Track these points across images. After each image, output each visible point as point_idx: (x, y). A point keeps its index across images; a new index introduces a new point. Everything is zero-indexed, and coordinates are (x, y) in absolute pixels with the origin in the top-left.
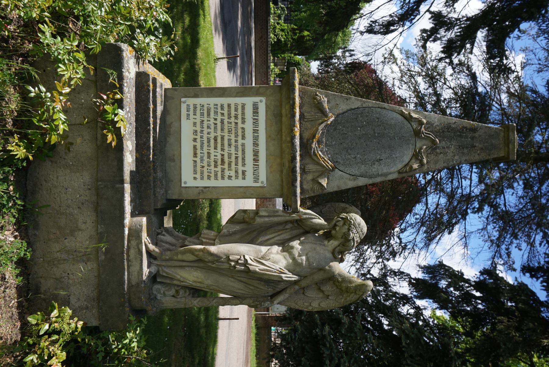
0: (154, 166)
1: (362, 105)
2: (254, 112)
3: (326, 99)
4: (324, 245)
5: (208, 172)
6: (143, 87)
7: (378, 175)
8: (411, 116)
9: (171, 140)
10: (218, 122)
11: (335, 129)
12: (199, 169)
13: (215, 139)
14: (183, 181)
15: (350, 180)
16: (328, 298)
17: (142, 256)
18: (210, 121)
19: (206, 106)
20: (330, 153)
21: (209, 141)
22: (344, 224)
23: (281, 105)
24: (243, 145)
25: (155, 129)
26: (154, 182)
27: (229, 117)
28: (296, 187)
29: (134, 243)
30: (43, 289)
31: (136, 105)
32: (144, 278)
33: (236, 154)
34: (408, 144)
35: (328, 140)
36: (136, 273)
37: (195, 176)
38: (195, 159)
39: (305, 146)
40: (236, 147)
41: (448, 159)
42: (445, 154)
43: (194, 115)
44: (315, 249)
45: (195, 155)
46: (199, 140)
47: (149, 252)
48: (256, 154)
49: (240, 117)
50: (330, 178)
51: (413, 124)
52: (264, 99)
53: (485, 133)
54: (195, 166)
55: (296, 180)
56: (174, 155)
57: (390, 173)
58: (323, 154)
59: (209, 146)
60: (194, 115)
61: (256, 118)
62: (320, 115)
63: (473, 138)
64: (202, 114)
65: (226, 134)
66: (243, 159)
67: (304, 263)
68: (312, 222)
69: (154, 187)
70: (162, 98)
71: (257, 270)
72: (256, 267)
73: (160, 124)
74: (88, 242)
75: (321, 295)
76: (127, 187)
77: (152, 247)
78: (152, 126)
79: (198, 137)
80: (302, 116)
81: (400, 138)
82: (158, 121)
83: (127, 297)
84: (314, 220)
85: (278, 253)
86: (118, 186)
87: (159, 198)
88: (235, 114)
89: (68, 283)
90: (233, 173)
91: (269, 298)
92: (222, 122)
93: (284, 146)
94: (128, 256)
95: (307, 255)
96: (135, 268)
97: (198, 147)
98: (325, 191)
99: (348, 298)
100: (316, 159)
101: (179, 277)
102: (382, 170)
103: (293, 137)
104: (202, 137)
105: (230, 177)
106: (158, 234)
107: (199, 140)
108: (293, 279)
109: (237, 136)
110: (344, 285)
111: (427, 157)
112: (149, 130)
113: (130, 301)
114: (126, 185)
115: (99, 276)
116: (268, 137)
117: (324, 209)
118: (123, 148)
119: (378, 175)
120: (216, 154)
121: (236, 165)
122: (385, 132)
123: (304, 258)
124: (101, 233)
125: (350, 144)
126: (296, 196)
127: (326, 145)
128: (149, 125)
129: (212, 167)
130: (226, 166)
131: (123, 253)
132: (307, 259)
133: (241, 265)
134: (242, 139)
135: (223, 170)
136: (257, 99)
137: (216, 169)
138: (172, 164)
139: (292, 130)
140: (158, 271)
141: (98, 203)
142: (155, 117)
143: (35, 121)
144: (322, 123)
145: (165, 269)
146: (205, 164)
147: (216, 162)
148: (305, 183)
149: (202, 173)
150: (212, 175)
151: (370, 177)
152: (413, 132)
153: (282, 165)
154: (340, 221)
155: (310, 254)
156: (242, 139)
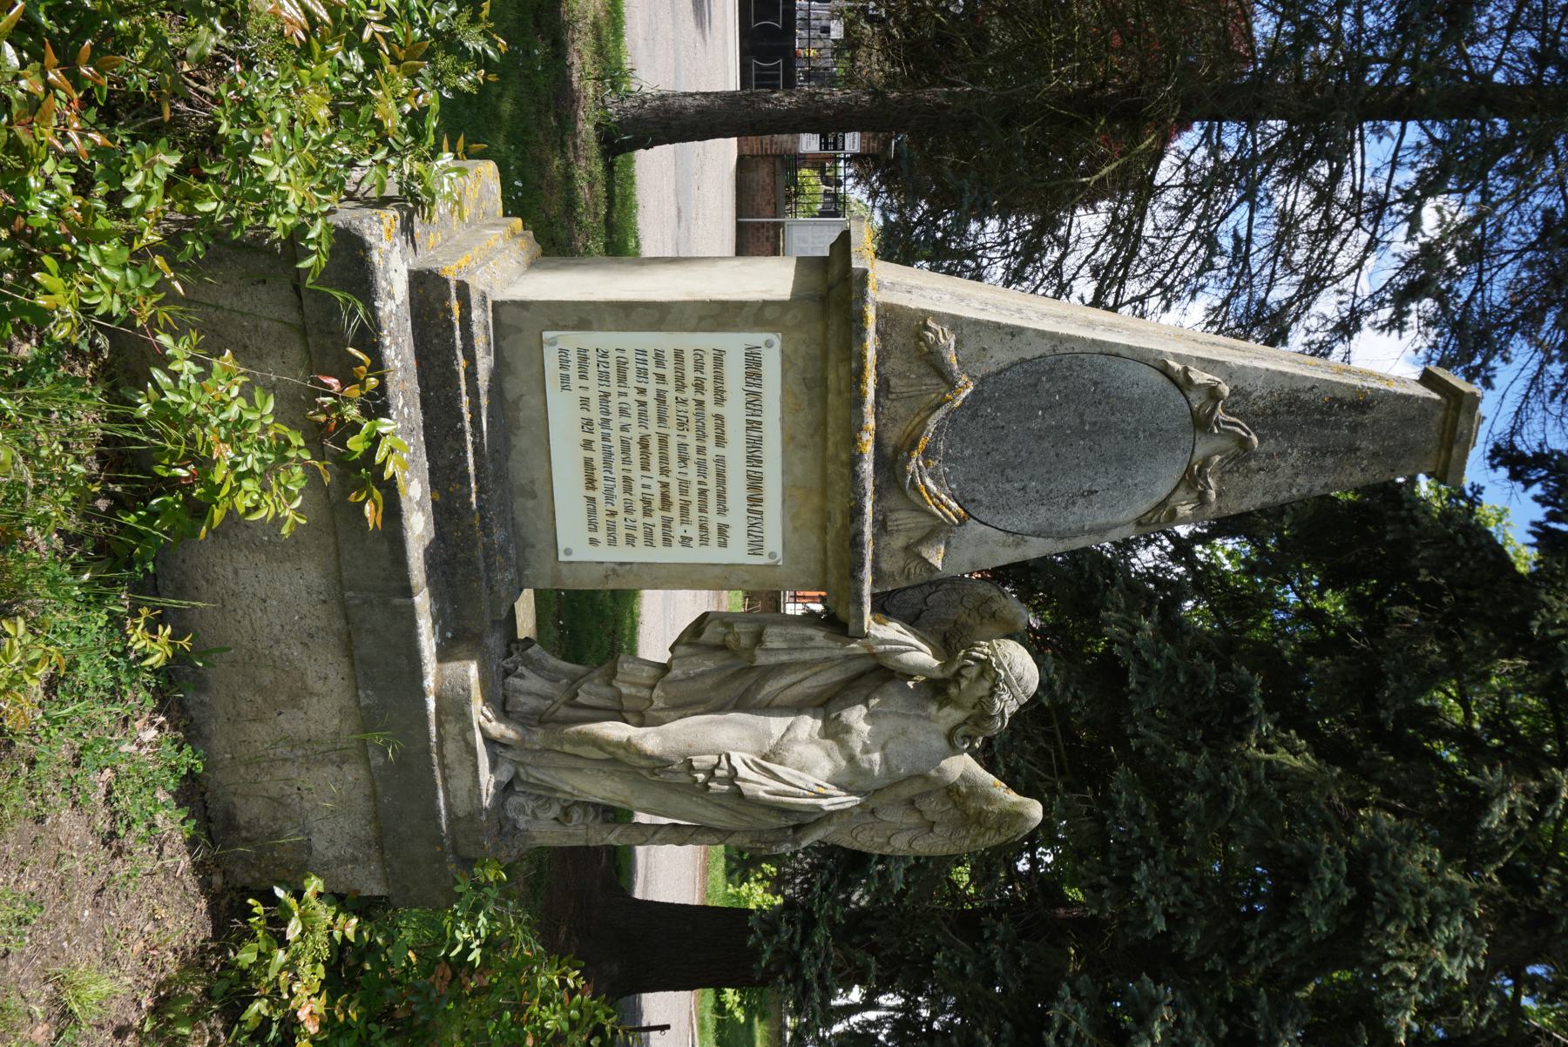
0: (482, 518)
1: (1054, 348)
2: (748, 375)
3: (952, 340)
4: (928, 718)
5: (627, 527)
6: (434, 313)
7: (1082, 531)
8: (1189, 380)
9: (522, 441)
10: (650, 398)
11: (974, 417)
12: (602, 518)
13: (644, 443)
14: (561, 547)
15: (1004, 545)
16: (932, 830)
17: (475, 756)
18: (626, 394)
19: (613, 355)
20: (956, 480)
21: (626, 449)
22: (981, 675)
23: (825, 356)
24: (720, 461)
25: (475, 422)
26: (486, 557)
27: (681, 387)
28: (862, 582)
29: (452, 728)
30: (242, 819)
31: (419, 365)
32: (486, 802)
33: (700, 483)
34: (1173, 450)
35: (951, 446)
36: (465, 793)
37: (593, 535)
38: (591, 494)
39: (890, 465)
40: (701, 465)
41: (1278, 485)
42: (1272, 471)
43: (581, 377)
44: (904, 732)
45: (591, 483)
46: (598, 444)
47: (490, 741)
48: (755, 484)
49: (709, 385)
50: (954, 542)
51: (1192, 396)
52: (776, 338)
53: (1393, 412)
54: (592, 512)
55: (863, 565)
56: (532, 482)
57: (1115, 526)
58: (937, 482)
59: (626, 461)
60: (581, 377)
61: (754, 389)
62: (935, 381)
63: (1354, 428)
64: (604, 377)
66: (721, 496)
67: (877, 768)
68: (898, 661)
69: (489, 568)
70: (487, 335)
71: (761, 794)
72: (758, 785)
73: (489, 405)
74: (336, 721)
75: (914, 819)
76: (422, 601)
77: (497, 729)
78: (467, 417)
79: (596, 437)
80: (883, 387)
81: (1151, 435)
82: (484, 401)
83: (447, 842)
84: (905, 656)
85: (811, 740)
86: (397, 601)
87: (503, 595)
88: (697, 379)
89: (302, 808)
90: (693, 531)
91: (790, 832)
92: (661, 398)
93: (831, 468)
94: (442, 756)
95: (883, 748)
96: (461, 782)
97: (598, 462)
98: (937, 576)
99: (980, 840)
100: (916, 499)
101: (568, 789)
102: (1095, 518)
103: (856, 459)
104: (605, 438)
105: (686, 541)
106: (507, 673)
107: (598, 444)
108: (848, 805)
109: (702, 436)
110: (972, 805)
111: (1220, 480)
112: (462, 431)
113: (455, 848)
114: (417, 599)
115: (374, 796)
116: (789, 440)
117: (934, 597)
118: (400, 509)
119: (1082, 531)
120: (646, 481)
121: (701, 510)
122: (1112, 419)
123: (876, 757)
124: (368, 708)
125: (1011, 453)
126: (861, 604)
127: (947, 458)
128: (461, 419)
129: (638, 514)
130: (675, 512)
131: (428, 751)
132: (885, 760)
133: (721, 780)
134: (717, 445)
135: (667, 523)
136: (757, 338)
137: (648, 520)
138: (530, 503)
139: (853, 441)
140: (517, 775)
141: (349, 635)
142: (474, 392)
143: (160, 470)
144: (938, 406)
145: (534, 773)
146: (619, 505)
147: (647, 502)
148: (885, 556)
149: (611, 529)
150: (639, 534)
151: (1061, 537)
152: (1189, 419)
153: (825, 516)
154: (969, 666)
155: (891, 745)
156: (717, 445)
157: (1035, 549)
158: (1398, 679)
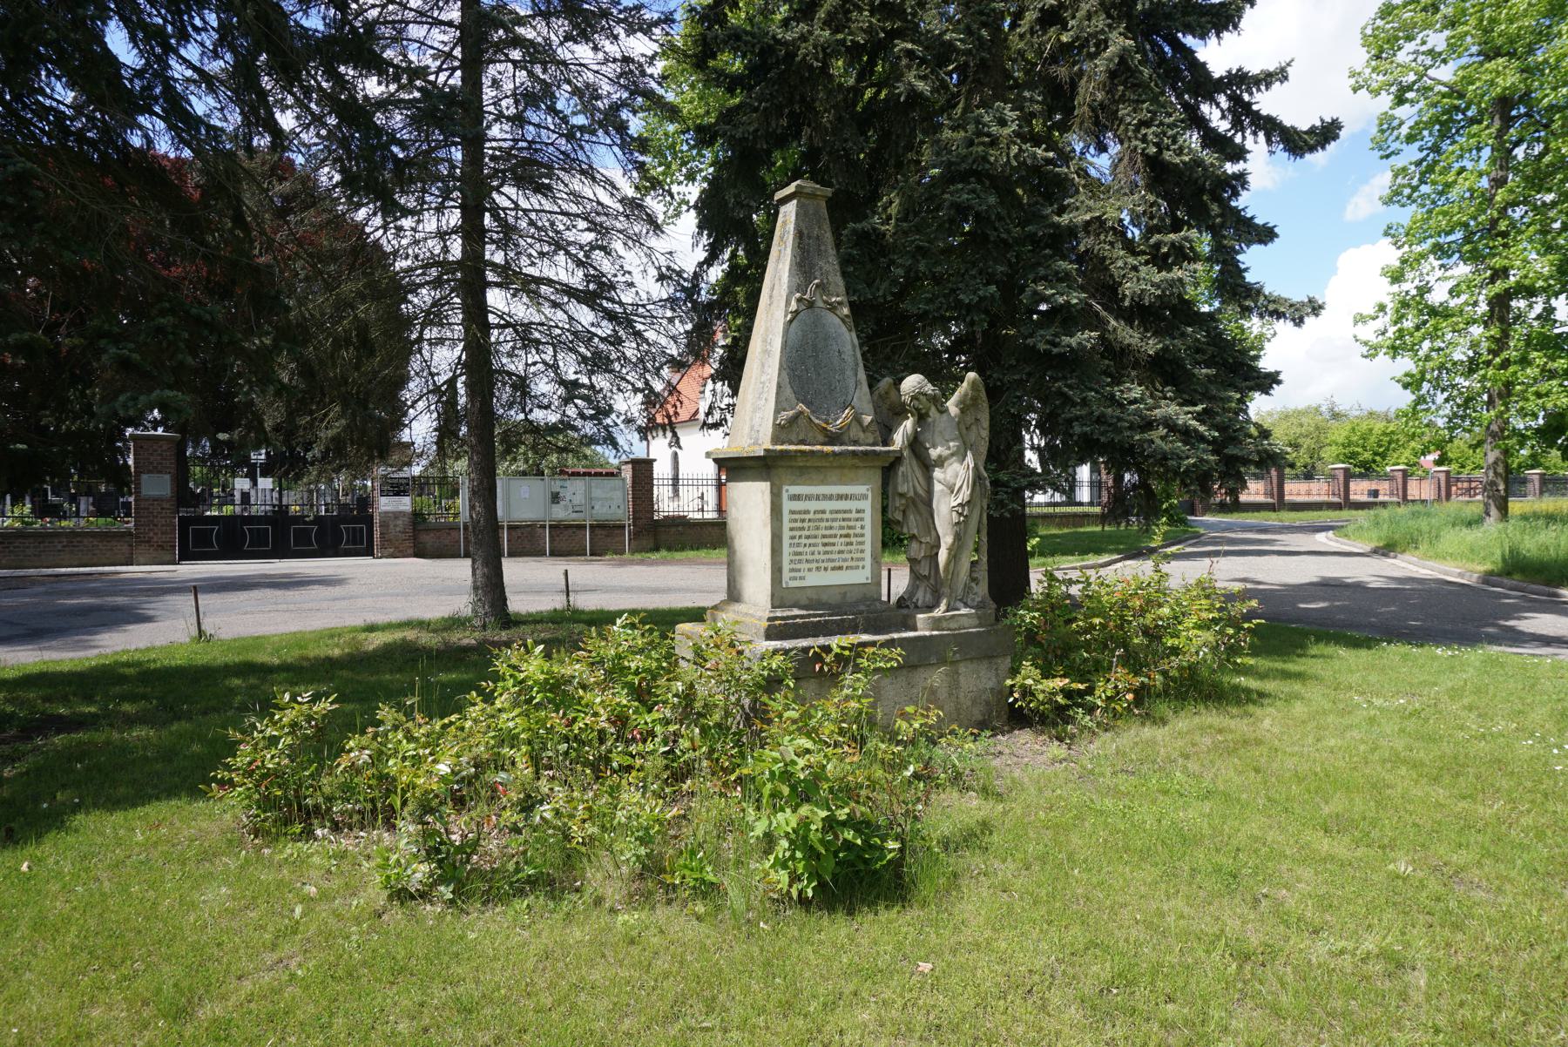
9: (824, 598)
12: (854, 564)
13: (825, 545)
21: (826, 553)
24: (831, 512)
29: (944, 624)
39: (832, 439)
40: (834, 520)
45: (840, 568)
48: (840, 497)
63: (809, 237)
64: (800, 561)
65: (820, 532)
72: (965, 494)
77: (943, 606)
80: (802, 442)
90: (859, 524)
92: (808, 537)
96: (966, 622)
115: (971, 659)
116: (823, 483)
135: (856, 535)
136: (785, 496)
142: (809, 616)
147: (847, 544)
149: (858, 559)
157: (862, 375)
158: (846, 141)
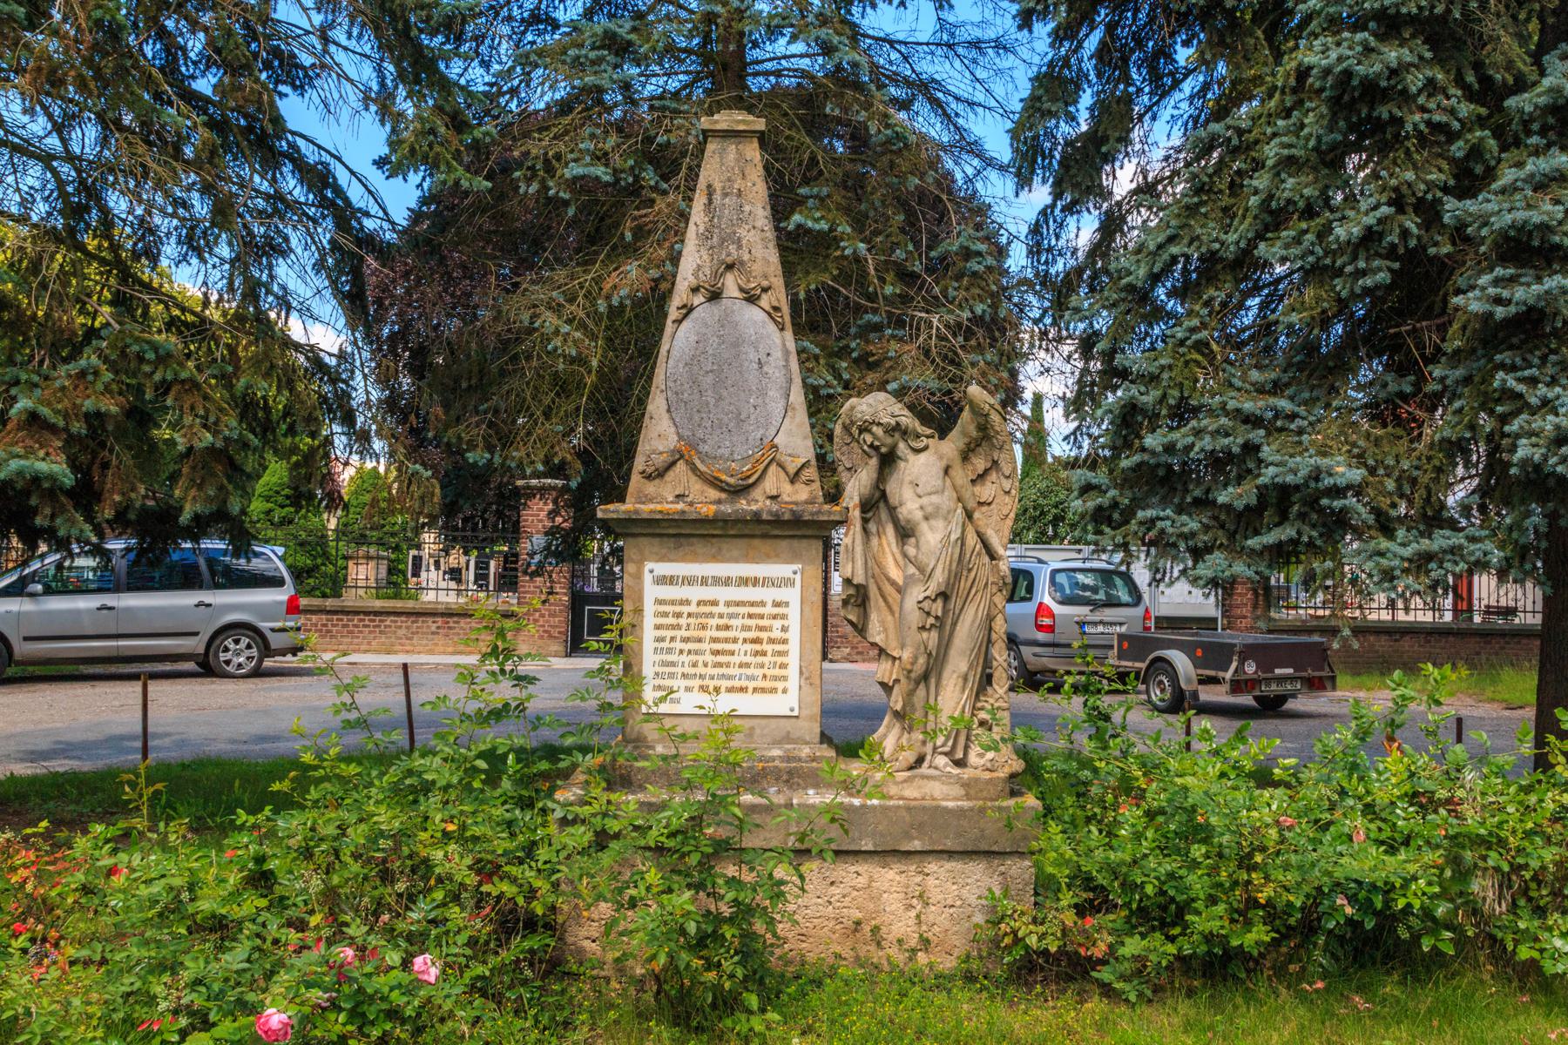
7: (786, 366)
12: (767, 684)
13: (717, 653)
21: (719, 665)
22: (869, 431)
24: (728, 604)
27: (679, 627)
40: (731, 616)
45: (742, 690)
48: (744, 582)
49: (678, 609)
54: (763, 690)
59: (728, 665)
64: (672, 676)
65: (708, 634)
66: (752, 604)
79: (712, 684)
90: (778, 624)
92: (686, 640)
104: (712, 678)
105: (784, 629)
107: (716, 683)
109: (711, 615)
116: (715, 558)
119: (786, 366)
129: (766, 660)
130: (764, 635)
135: (772, 641)
147: (757, 653)
149: (776, 678)
150: (779, 660)
153: (765, 536)
157: (798, 396)
